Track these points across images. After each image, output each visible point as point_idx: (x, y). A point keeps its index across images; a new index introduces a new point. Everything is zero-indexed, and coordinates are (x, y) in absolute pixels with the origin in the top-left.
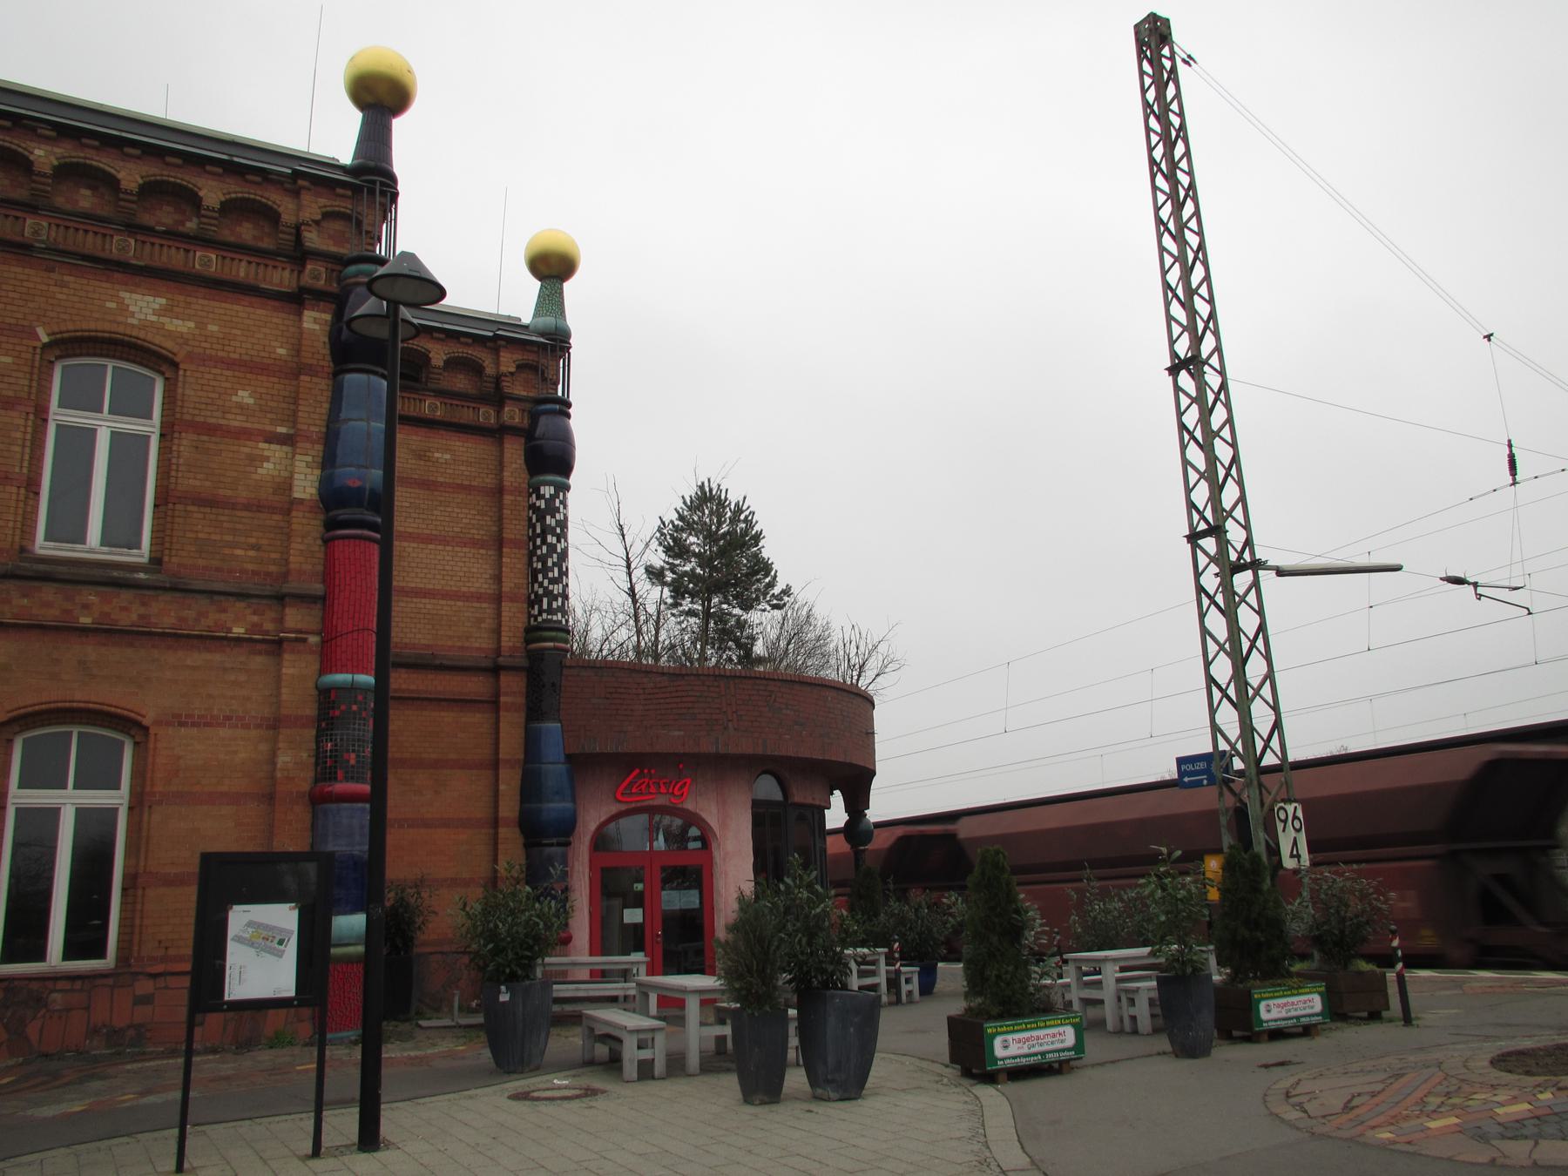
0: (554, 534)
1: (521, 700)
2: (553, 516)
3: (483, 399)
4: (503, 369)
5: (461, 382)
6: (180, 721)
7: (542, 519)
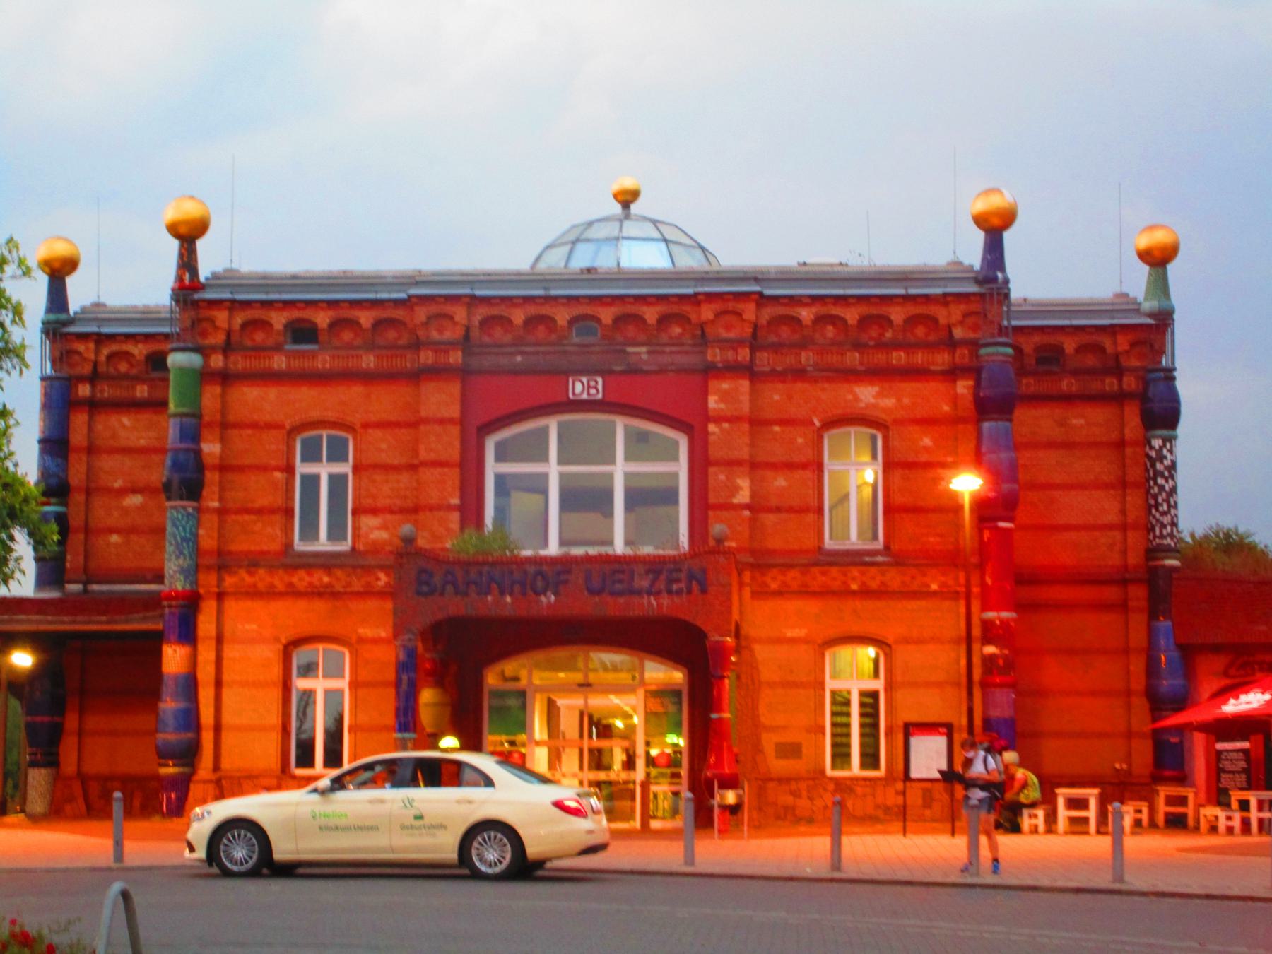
0: (1162, 475)
1: (1144, 604)
2: (1162, 462)
3: (1106, 372)
4: (1120, 349)
5: (1091, 361)
6: (907, 641)
7: (1153, 465)
